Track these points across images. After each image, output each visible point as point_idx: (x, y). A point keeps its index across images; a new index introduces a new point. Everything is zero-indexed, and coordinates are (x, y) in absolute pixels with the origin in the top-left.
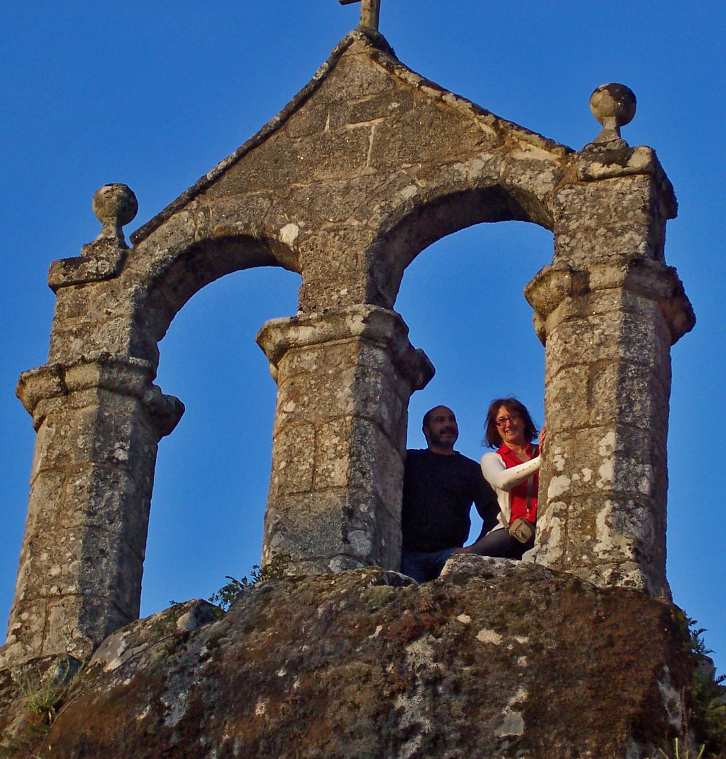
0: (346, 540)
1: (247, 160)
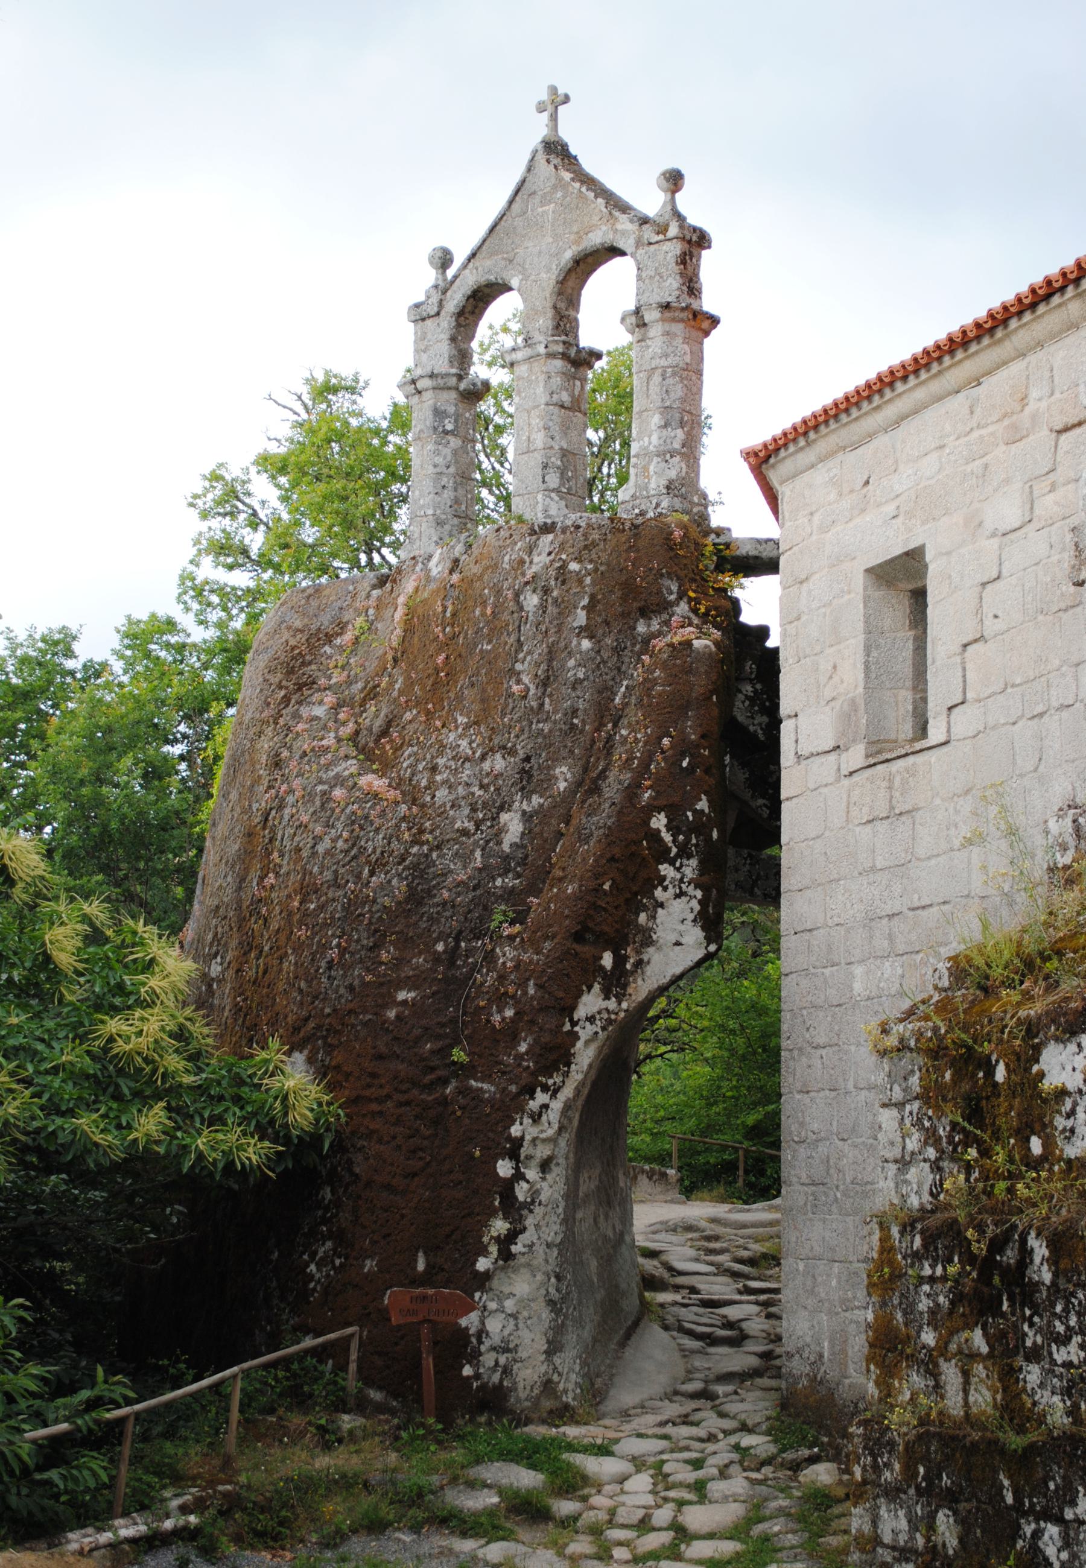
0: (544, 482)
1: (494, 234)
